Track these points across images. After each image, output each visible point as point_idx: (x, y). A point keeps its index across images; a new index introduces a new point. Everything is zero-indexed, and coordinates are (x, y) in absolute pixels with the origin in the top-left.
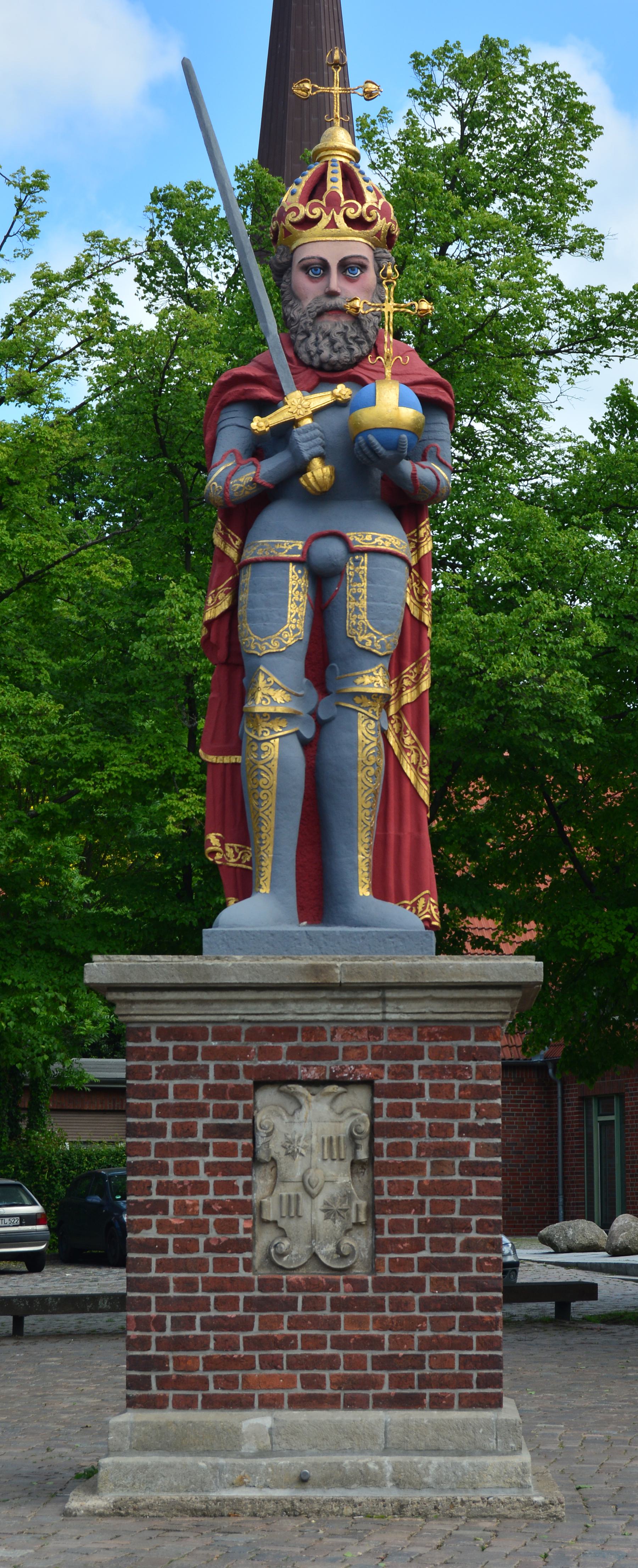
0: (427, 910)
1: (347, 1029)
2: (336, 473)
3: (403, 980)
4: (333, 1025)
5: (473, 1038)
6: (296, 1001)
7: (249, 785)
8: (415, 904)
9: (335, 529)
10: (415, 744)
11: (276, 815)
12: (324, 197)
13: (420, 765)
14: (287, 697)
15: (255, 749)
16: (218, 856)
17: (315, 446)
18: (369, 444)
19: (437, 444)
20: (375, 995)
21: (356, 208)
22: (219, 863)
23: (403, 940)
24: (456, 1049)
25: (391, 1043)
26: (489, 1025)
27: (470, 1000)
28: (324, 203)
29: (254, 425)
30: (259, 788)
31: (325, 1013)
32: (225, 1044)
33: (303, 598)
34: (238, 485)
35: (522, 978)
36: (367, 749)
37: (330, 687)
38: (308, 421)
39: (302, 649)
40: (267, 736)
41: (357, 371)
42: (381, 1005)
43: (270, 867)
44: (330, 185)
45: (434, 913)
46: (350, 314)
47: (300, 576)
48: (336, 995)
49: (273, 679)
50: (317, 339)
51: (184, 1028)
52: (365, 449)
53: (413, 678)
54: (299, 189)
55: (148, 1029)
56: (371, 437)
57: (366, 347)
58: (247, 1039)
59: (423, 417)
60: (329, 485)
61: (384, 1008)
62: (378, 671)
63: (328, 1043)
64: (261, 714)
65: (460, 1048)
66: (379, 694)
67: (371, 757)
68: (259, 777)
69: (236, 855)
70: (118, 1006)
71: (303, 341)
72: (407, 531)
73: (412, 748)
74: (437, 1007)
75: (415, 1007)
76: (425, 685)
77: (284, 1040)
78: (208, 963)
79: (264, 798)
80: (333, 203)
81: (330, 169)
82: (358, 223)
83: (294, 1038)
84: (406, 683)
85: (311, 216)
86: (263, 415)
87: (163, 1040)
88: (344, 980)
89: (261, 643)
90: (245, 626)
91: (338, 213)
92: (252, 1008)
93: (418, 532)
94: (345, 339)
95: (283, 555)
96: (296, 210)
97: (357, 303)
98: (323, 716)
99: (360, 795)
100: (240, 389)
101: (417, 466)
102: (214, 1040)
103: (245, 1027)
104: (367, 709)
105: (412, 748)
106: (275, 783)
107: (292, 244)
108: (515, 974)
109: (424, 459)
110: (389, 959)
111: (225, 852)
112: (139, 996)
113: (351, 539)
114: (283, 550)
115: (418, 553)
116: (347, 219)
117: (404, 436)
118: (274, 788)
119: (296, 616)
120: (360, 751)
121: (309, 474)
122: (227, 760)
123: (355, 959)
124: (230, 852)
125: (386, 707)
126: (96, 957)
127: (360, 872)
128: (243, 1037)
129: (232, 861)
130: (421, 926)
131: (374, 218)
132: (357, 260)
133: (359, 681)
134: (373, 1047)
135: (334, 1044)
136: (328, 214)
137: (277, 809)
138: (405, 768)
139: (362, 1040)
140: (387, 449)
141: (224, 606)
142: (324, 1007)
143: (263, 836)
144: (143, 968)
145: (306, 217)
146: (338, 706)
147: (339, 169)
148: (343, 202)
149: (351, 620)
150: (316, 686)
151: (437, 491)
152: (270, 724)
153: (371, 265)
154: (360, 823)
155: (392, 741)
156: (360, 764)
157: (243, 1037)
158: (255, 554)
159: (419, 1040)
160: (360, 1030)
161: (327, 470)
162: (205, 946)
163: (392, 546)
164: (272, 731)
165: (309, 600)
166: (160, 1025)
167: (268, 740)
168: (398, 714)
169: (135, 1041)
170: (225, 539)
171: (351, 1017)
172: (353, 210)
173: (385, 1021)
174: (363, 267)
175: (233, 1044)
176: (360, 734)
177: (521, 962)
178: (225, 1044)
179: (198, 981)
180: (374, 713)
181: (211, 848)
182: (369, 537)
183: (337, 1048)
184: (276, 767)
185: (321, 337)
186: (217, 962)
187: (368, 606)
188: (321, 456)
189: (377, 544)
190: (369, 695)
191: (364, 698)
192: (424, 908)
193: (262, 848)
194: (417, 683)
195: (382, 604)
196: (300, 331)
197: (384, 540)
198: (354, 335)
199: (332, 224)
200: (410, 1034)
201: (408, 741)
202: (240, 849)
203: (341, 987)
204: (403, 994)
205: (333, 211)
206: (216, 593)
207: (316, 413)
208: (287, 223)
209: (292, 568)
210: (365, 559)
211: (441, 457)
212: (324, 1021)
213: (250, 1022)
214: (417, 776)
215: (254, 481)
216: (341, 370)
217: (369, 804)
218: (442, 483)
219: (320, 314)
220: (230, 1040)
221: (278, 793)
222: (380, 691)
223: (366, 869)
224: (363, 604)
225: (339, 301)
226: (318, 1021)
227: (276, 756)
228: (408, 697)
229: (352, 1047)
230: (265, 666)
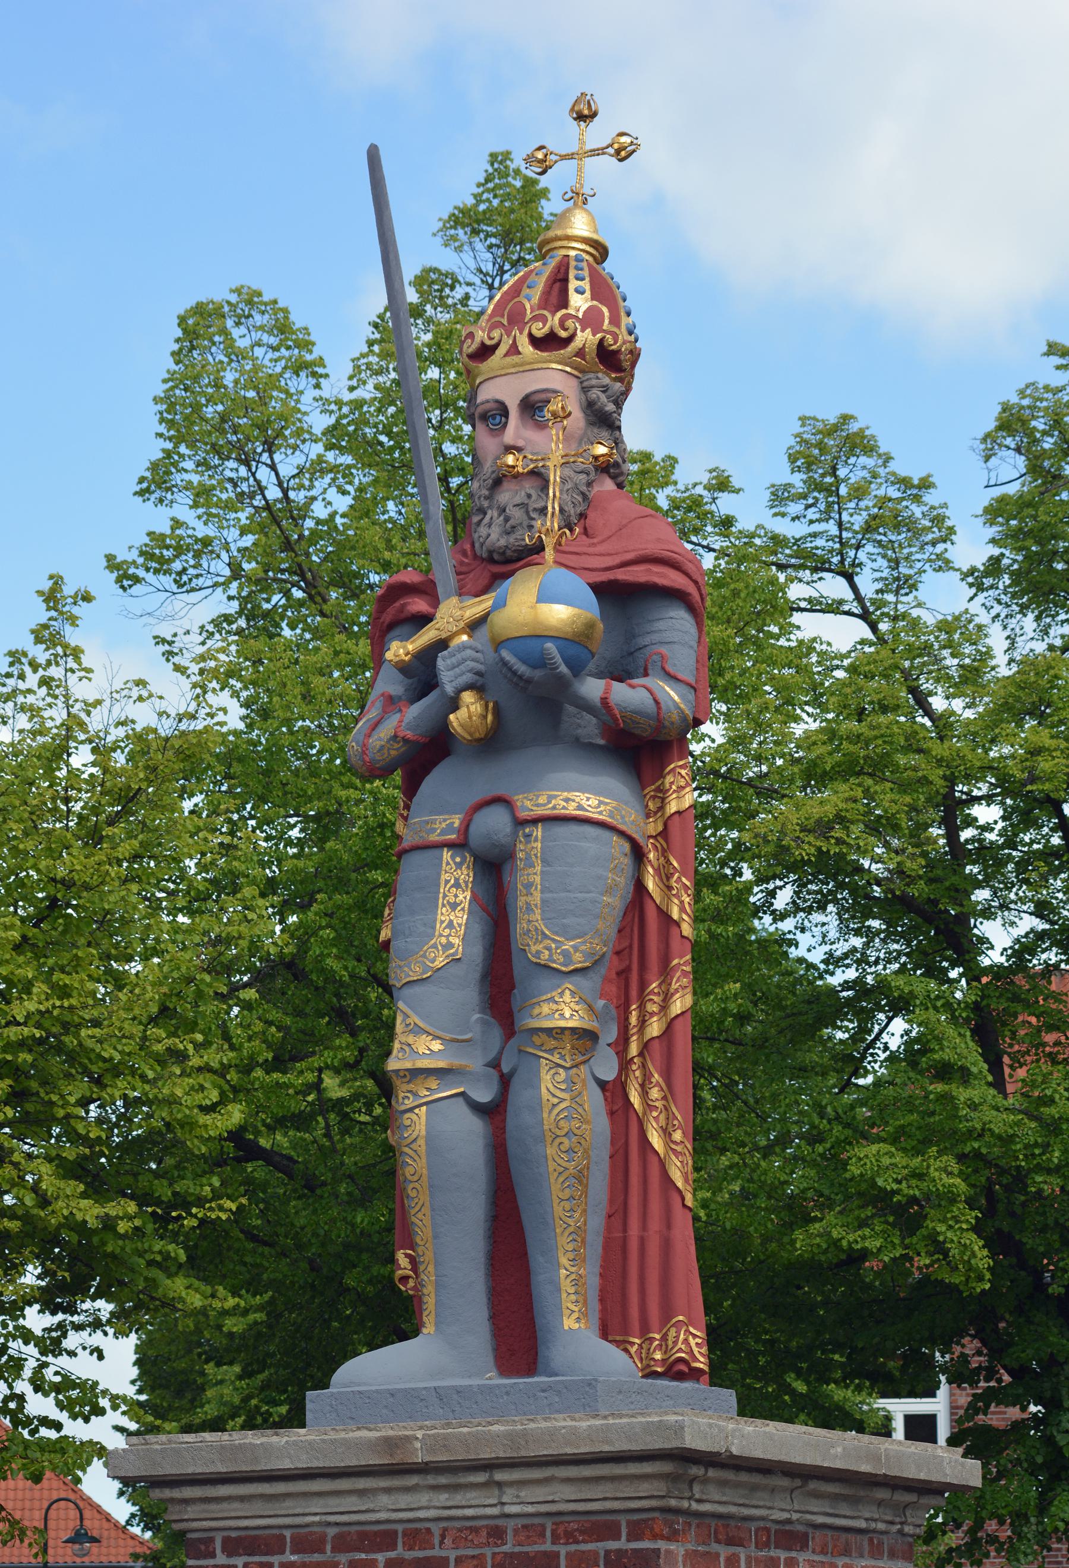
1: (460, 1530)
4: (444, 1524)
5: (624, 1537)
6: (388, 1491)
8: (664, 1338)
10: (664, 1098)
16: (411, 1283)
17: (463, 673)
19: (664, 649)
20: (481, 1478)
22: (411, 1292)
23: (559, 1393)
24: (602, 1554)
25: (517, 1549)
26: (644, 1516)
27: (613, 1479)
31: (428, 1508)
32: (308, 1558)
34: (378, 744)
36: (556, 1111)
40: (409, 1103)
42: (496, 1492)
43: (433, 1295)
47: (459, 866)
48: (431, 1480)
49: (415, 1019)
51: (256, 1537)
55: (212, 1540)
58: (333, 1550)
61: (500, 1497)
62: (562, 994)
63: (436, 1552)
64: (397, 1071)
65: (607, 1553)
66: (563, 1030)
67: (562, 1123)
70: (171, 1508)
74: (569, 1492)
75: (540, 1493)
77: (380, 1550)
79: (413, 1194)
82: (549, 342)
83: (393, 1547)
85: (488, 342)
87: (229, 1555)
88: (427, 1459)
95: (434, 838)
99: (552, 1181)
102: (293, 1553)
103: (332, 1532)
104: (551, 1051)
106: (425, 1171)
109: (646, 674)
112: (188, 1492)
113: (519, 804)
117: (549, 645)
118: (425, 1178)
120: (545, 1115)
123: (448, 1425)
127: (564, 1295)
128: (329, 1547)
131: (571, 331)
133: (536, 1011)
134: (494, 1554)
135: (443, 1553)
137: (433, 1210)
139: (478, 1546)
142: (423, 1498)
145: (483, 344)
146: (520, 1051)
152: (411, 1086)
157: (329, 1547)
159: (553, 1543)
160: (475, 1530)
162: (309, 1416)
163: (580, 807)
164: (415, 1095)
165: (474, 897)
166: (226, 1534)
167: (411, 1110)
168: (641, 1054)
169: (197, 1558)
171: (459, 1513)
175: (317, 1557)
176: (544, 1090)
178: (308, 1558)
179: (244, 1468)
180: (562, 1057)
181: (400, 1273)
182: (542, 800)
183: (447, 1559)
184: (424, 1147)
187: (543, 901)
189: (554, 808)
190: (549, 1031)
191: (544, 1036)
194: (664, 1007)
195: (563, 895)
197: (567, 800)
199: (514, 350)
200: (543, 1535)
201: (655, 1093)
205: (516, 331)
209: (446, 855)
210: (538, 831)
213: (337, 1524)
217: (568, 1193)
220: (313, 1552)
221: (431, 1186)
222: (562, 1024)
224: (537, 897)
226: (420, 1520)
227: (423, 1133)
229: (467, 1557)
230: (405, 1003)
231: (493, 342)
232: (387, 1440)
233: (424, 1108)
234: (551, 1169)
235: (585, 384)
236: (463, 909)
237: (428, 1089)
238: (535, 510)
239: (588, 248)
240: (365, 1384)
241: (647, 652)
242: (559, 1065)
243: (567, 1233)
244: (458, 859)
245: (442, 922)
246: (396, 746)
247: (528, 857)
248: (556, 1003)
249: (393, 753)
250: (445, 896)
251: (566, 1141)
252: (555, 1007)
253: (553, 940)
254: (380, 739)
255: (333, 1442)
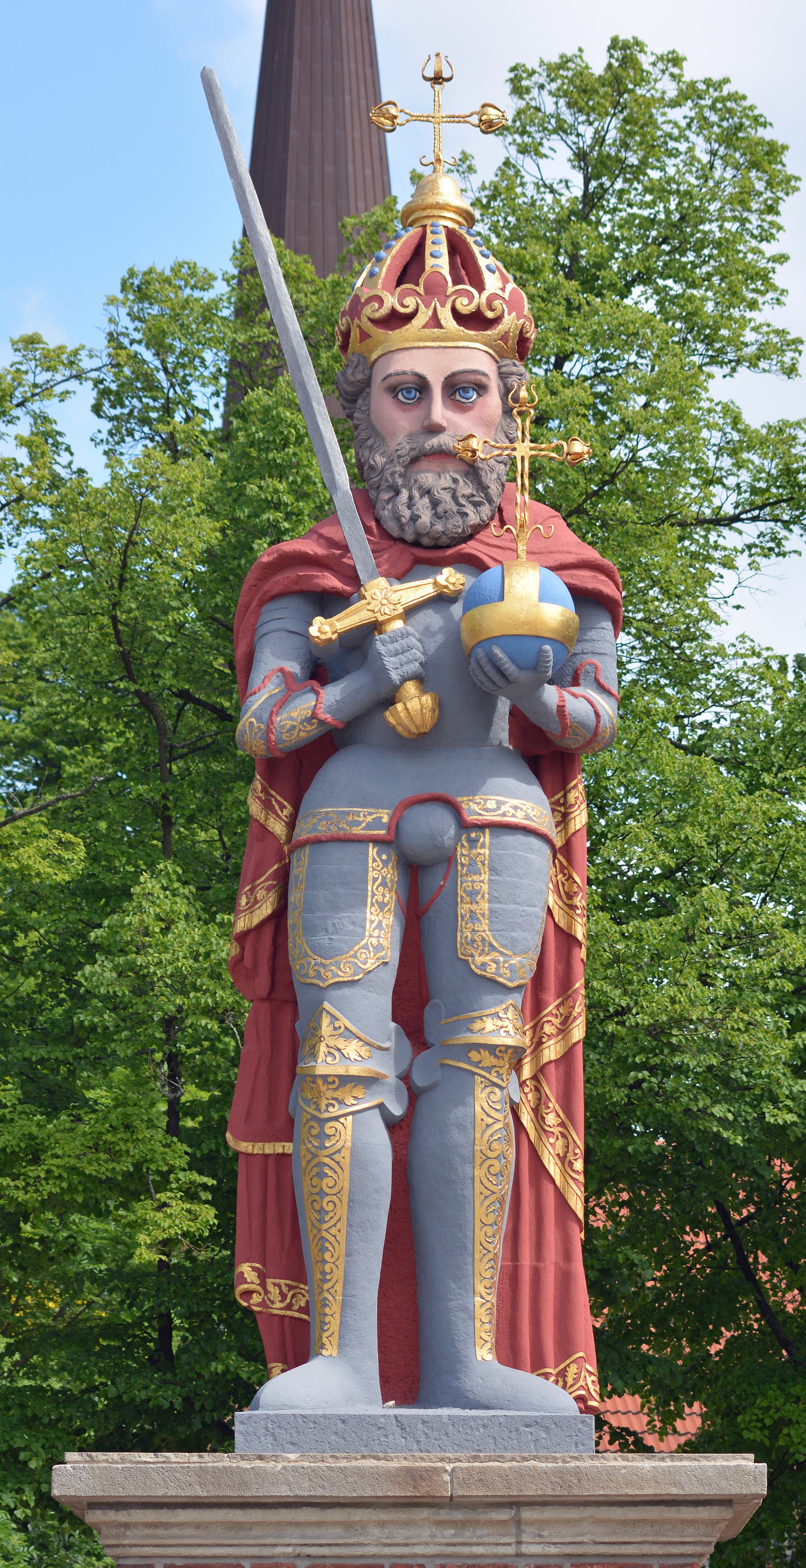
0: (581, 1383)
2: (440, 705)
3: (550, 1492)
6: (382, 1524)
7: (304, 1187)
8: (563, 1374)
9: (439, 790)
11: (348, 1234)
12: (422, 281)
13: (570, 1156)
14: (364, 1051)
15: (314, 1132)
16: (256, 1299)
17: (409, 662)
18: (493, 661)
19: (596, 660)
20: (505, 1515)
21: (471, 297)
22: (255, 1308)
23: (547, 1429)
28: (421, 290)
29: (313, 631)
30: (322, 1194)
33: (390, 898)
35: (733, 1489)
36: (489, 1132)
37: (430, 1035)
38: (398, 624)
39: (390, 976)
40: (335, 1111)
41: (471, 547)
43: (337, 1316)
44: (429, 262)
45: (591, 1387)
46: (461, 459)
47: (385, 863)
49: (344, 1022)
50: (411, 498)
52: (488, 668)
53: (557, 1022)
54: (383, 271)
56: (497, 651)
57: (486, 510)
59: (577, 618)
60: (429, 724)
61: (518, 1535)
62: (506, 1010)
64: (325, 1077)
66: (508, 1047)
67: (495, 1145)
68: (322, 1175)
69: (283, 1296)
71: (388, 501)
72: (549, 794)
73: (557, 1130)
75: (567, 1534)
76: (578, 1032)
78: (245, 1465)
80: (435, 290)
81: (430, 238)
84: (548, 1029)
86: (327, 614)
89: (324, 966)
90: (296, 942)
91: (443, 305)
92: (313, 1535)
93: (565, 796)
94: (454, 497)
95: (358, 831)
96: (380, 300)
97: (474, 443)
98: (419, 1080)
99: (477, 1204)
100: (291, 574)
101: (565, 693)
104: (488, 1069)
105: (557, 1130)
106: (346, 1184)
107: (372, 351)
108: (724, 1483)
109: (576, 682)
110: (526, 1459)
111: (266, 1292)
112: (138, 1516)
113: (464, 806)
114: (359, 823)
115: (566, 828)
116: (457, 315)
117: (547, 647)
118: (346, 1192)
119: (379, 926)
120: (478, 1135)
121: (399, 706)
122: (269, 1148)
123: (475, 1458)
124: (274, 1292)
125: (517, 1067)
126: (70, 1456)
127: (478, 1324)
129: (277, 1307)
130: (573, 1408)
131: (498, 313)
132: (472, 377)
133: (477, 1026)
136: (427, 306)
137: (349, 1225)
138: (545, 1162)
140: (521, 668)
141: (266, 910)
142: (425, 1533)
143: (327, 1268)
144: (146, 1473)
145: (393, 311)
146: (443, 1065)
147: (443, 237)
148: (451, 289)
149: (464, 933)
150: (408, 1035)
151: (596, 733)
152: (338, 1094)
153: (494, 384)
154: (478, 1247)
155: (526, 1119)
156: (478, 1155)
158: (314, 829)
161: (427, 700)
163: (527, 817)
164: (341, 1102)
165: (398, 900)
167: (336, 1119)
168: (535, 1078)
170: (267, 805)
171: (466, 1550)
172: (465, 301)
173: (519, 1555)
174: (481, 388)
176: (478, 1109)
177: (733, 1463)
179: (229, 1493)
180: (499, 1075)
184: (348, 1159)
185: (416, 494)
186: (258, 1463)
187: (491, 911)
188: (419, 679)
189: (504, 815)
190: (492, 1049)
191: (485, 1054)
192: (576, 1380)
193: (327, 1286)
194: (564, 1029)
195: (513, 906)
196: (384, 485)
197: (516, 808)
198: (468, 491)
199: (435, 321)
201: (551, 1119)
202: (291, 1288)
203: (452, 1503)
204: (548, 1514)
205: (435, 302)
206: (252, 890)
207: (410, 612)
208: (364, 319)
209: (372, 851)
210: (486, 838)
211: (602, 680)
212: (424, 1556)
214: (564, 1173)
215: (314, 716)
216: (449, 546)
217: (491, 1218)
218: (605, 721)
219: (414, 460)
221: (350, 1200)
222: (509, 1042)
223: (486, 1319)
225: (444, 440)
226: (415, 1556)
227: (349, 1144)
228: (552, 1051)
231: (408, 311)
232: (409, 1471)
233: (350, 1118)
234: (477, 1191)
235: (504, 369)
236: (389, 910)
237: (355, 1098)
238: (464, 496)
239: (460, 219)
240: (298, 1407)
241: (578, 661)
242: (495, 1084)
243: (486, 1259)
244: (384, 857)
245: (372, 922)
246: (309, 728)
247: (472, 863)
248: (500, 1019)
249: (302, 734)
250: (373, 895)
251: (495, 1162)
252: (499, 1023)
253: (502, 953)
254: (292, 719)
255: (342, 1470)
